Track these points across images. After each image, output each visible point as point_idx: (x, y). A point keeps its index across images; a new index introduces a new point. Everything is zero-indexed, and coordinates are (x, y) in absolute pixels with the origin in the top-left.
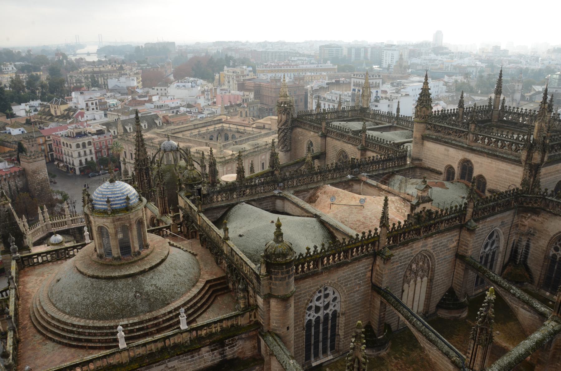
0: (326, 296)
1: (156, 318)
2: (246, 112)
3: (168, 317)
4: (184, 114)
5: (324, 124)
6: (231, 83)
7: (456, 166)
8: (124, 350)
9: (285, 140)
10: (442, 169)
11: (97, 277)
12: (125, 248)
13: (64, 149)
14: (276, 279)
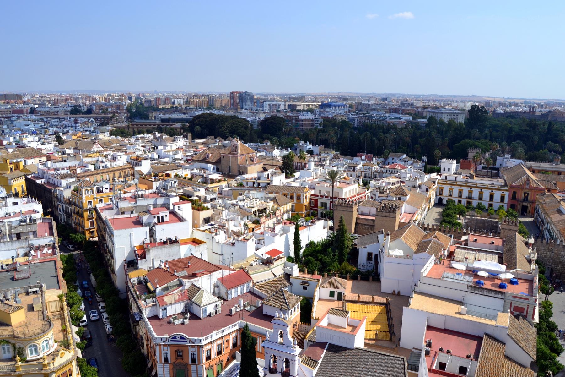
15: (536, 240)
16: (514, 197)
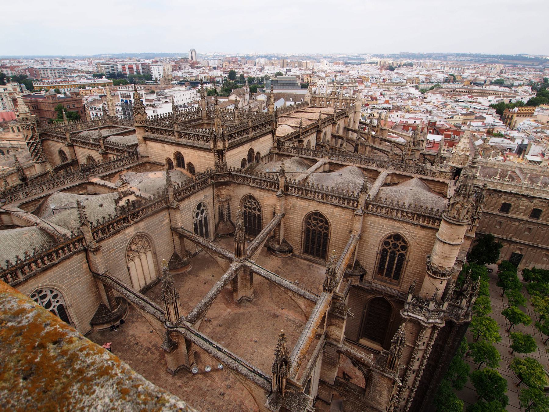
0: (45, 296)
2: (18, 127)
5: (68, 136)
7: (172, 158)
9: (37, 153)
10: (164, 162)
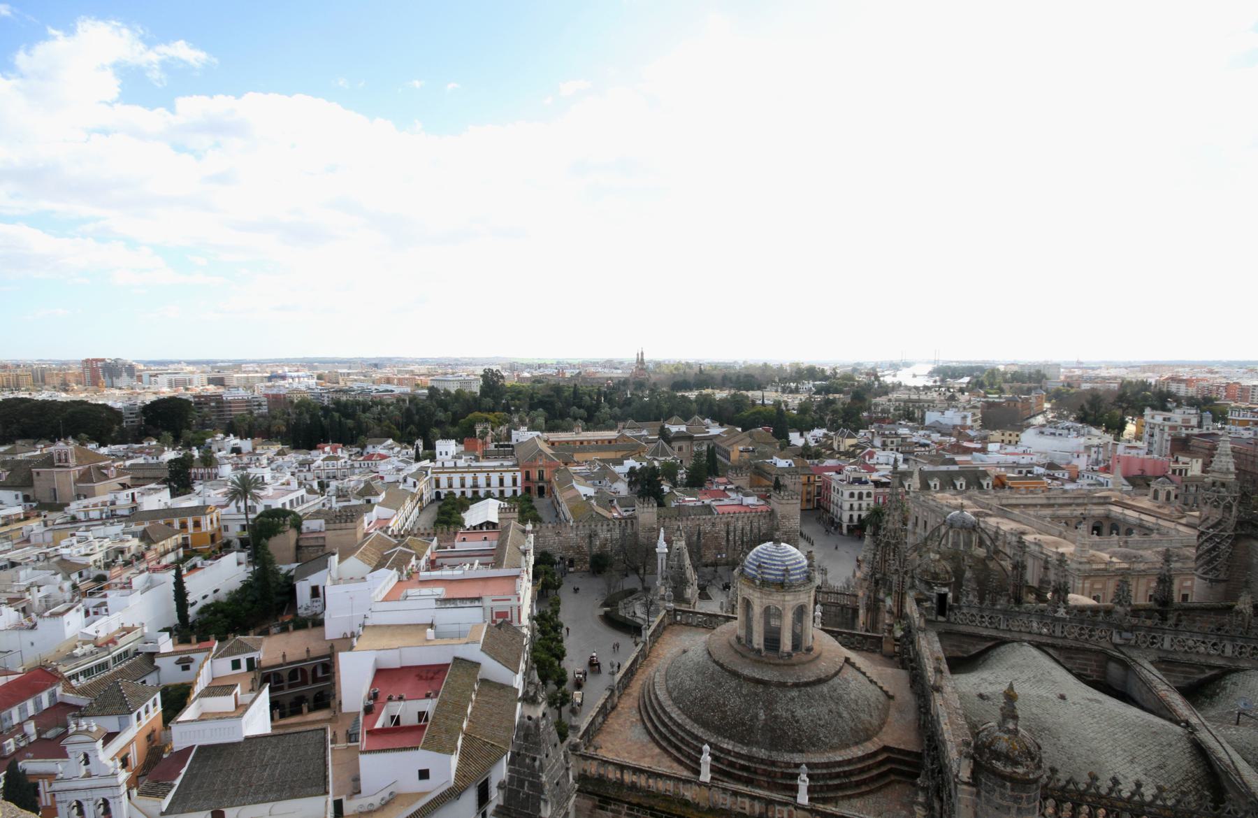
1: (773, 763)
2: (1169, 493)
3: (790, 771)
4: (1038, 477)
6: (1156, 438)
8: (705, 784)
9: (1214, 559)
11: (722, 666)
12: (773, 641)
13: (834, 496)
14: (988, 801)
15: (534, 526)
16: (527, 477)
